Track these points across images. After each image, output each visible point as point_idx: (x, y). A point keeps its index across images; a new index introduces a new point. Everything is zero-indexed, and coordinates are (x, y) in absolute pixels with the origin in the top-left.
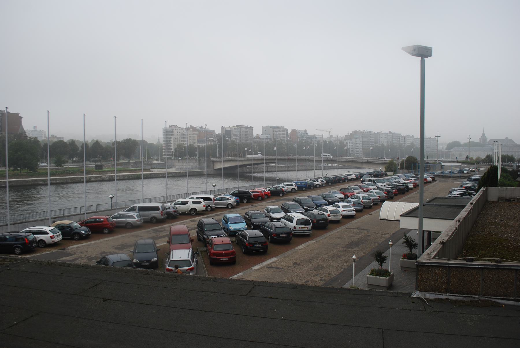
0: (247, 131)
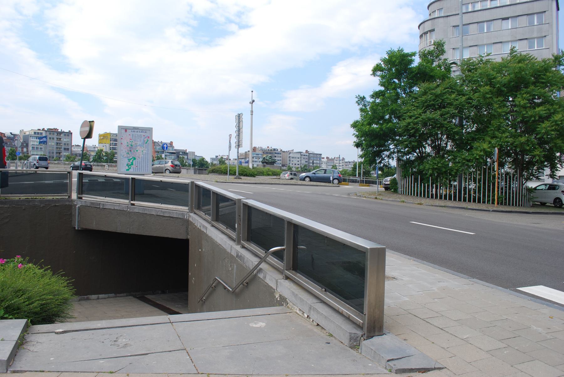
0: (60, 139)
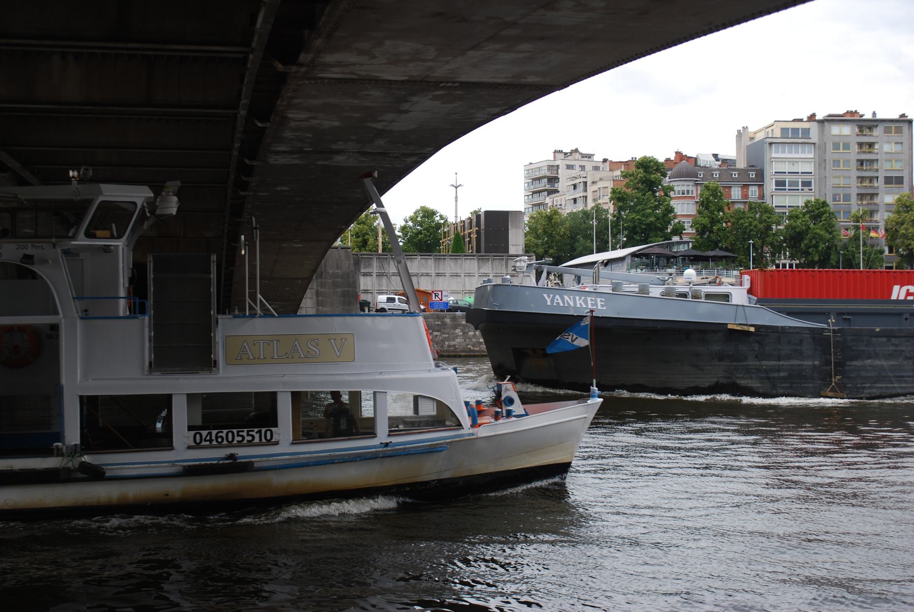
0: (871, 145)
